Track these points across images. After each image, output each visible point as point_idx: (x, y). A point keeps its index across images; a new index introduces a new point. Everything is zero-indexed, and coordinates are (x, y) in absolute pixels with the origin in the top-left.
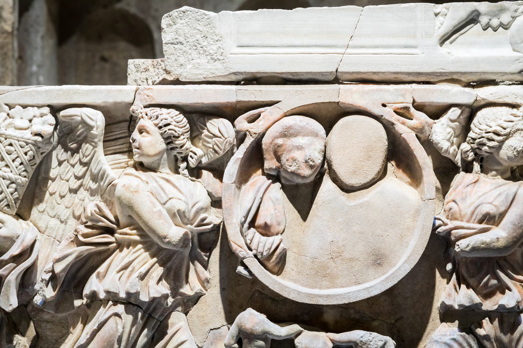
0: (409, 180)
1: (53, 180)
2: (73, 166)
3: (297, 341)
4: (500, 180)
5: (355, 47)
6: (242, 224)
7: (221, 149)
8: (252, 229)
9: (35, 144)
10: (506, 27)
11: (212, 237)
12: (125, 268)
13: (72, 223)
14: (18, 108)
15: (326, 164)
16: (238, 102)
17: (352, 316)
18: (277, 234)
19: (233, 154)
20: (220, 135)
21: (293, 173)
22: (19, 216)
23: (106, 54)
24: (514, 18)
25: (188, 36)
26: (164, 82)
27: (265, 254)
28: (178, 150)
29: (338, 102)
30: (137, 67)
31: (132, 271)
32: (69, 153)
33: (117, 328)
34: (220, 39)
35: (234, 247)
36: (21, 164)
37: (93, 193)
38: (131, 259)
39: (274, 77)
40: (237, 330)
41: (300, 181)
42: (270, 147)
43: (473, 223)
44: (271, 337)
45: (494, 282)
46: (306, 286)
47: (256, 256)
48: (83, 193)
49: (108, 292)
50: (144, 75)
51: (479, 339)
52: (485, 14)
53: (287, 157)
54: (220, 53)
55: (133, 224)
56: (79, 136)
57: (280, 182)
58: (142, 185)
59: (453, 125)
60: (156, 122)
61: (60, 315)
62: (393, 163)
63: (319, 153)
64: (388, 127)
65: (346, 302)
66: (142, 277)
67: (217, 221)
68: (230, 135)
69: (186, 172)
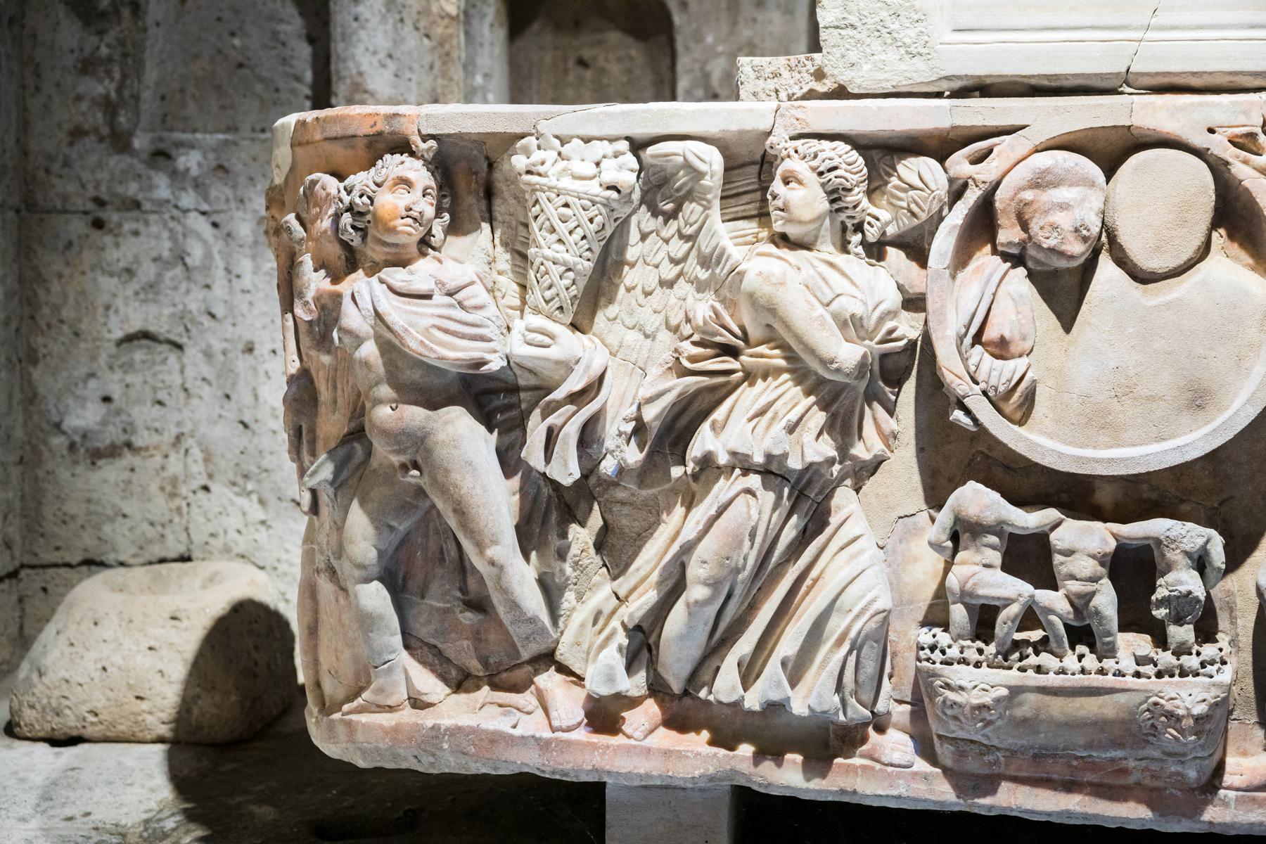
0: (1251, 261)
1: (632, 265)
2: (667, 241)
3: (1054, 537)
5: (1161, 28)
6: (961, 339)
7: (923, 211)
8: (978, 348)
9: (607, 204)
11: (903, 360)
12: (761, 413)
13: (665, 337)
14: (576, 141)
15: (1104, 234)
16: (954, 128)
17: (1145, 496)
18: (1020, 356)
19: (941, 219)
20: (921, 185)
21: (1052, 250)
22: (574, 326)
23: (587, 54)
25: (865, 13)
26: (811, 95)
27: (1001, 389)
28: (849, 213)
29: (1129, 127)
30: (757, 70)
31: (773, 418)
32: (661, 218)
33: (748, 513)
34: (923, 17)
35: (948, 377)
36: (584, 237)
37: (701, 287)
39: (1015, 83)
40: (952, 517)
41: (1062, 264)
42: (1010, 205)
44: (1010, 529)
46: (1070, 444)
47: (985, 393)
48: (683, 287)
49: (734, 454)
50: (771, 84)
53: (1042, 223)
54: (923, 42)
55: (772, 338)
56: (678, 190)
57: (1025, 267)
58: (791, 272)
60: (814, 163)
61: (645, 493)
62: (1222, 231)
63: (1097, 215)
64: (1219, 169)
65: (1143, 470)
66: (791, 429)
67: (914, 334)
68: (939, 186)
69: (860, 249)
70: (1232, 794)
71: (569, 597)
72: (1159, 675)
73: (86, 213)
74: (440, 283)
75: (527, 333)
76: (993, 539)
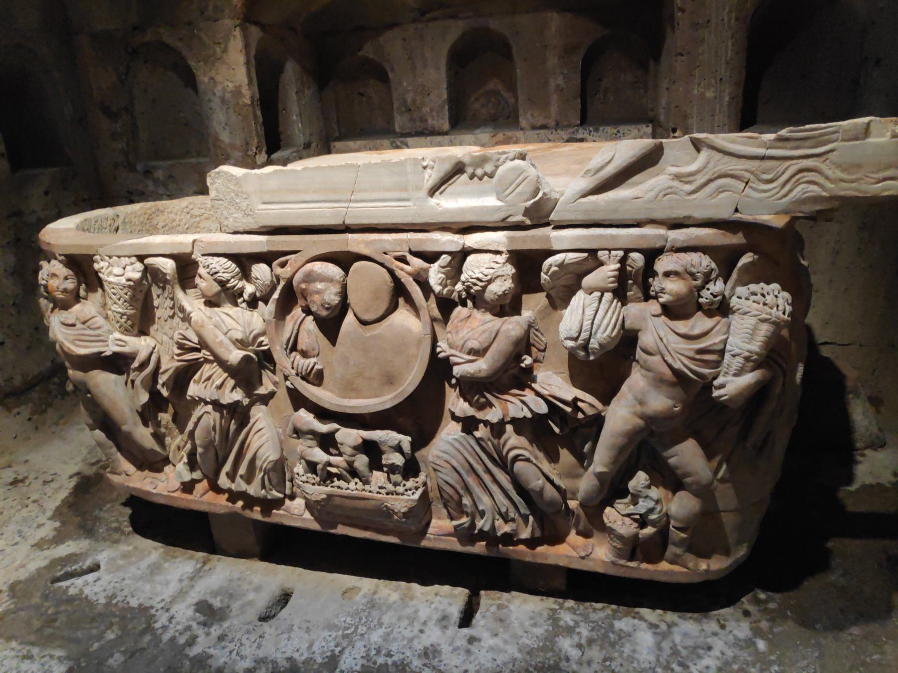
1: (157, 308)
4: (488, 316)
8: (294, 353)
9: (130, 287)
10: (491, 176)
18: (314, 357)
24: (497, 167)
38: (211, 373)
43: (464, 353)
45: (483, 400)
51: (478, 441)
52: (470, 165)
59: (443, 270)
64: (391, 272)
66: (220, 387)
70: (432, 536)
71: (168, 440)
72: (387, 494)
73: (126, 197)
76: (310, 436)
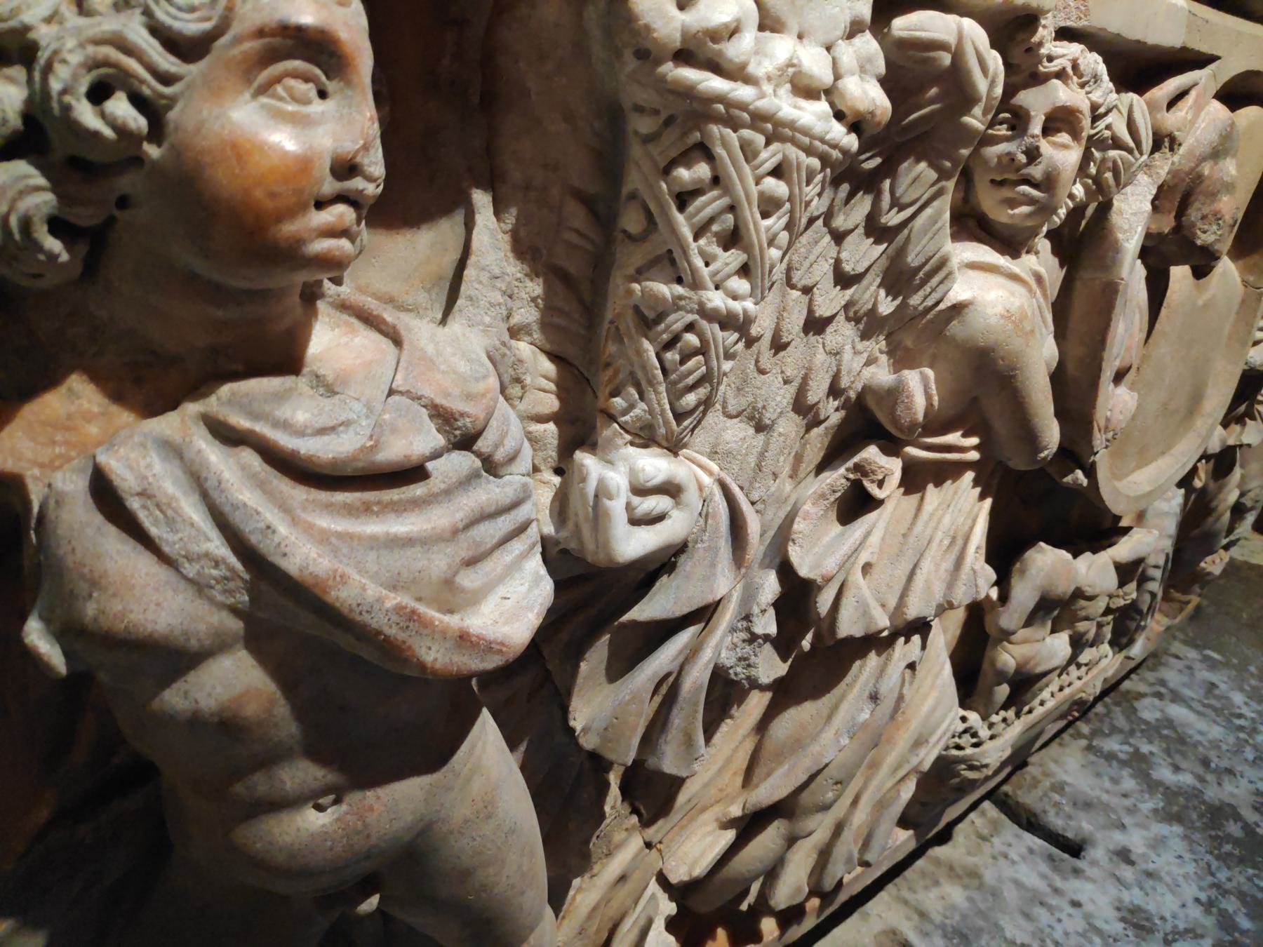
2: (839, 237)
20: (1132, 144)
74: (443, 417)
75: (636, 500)
